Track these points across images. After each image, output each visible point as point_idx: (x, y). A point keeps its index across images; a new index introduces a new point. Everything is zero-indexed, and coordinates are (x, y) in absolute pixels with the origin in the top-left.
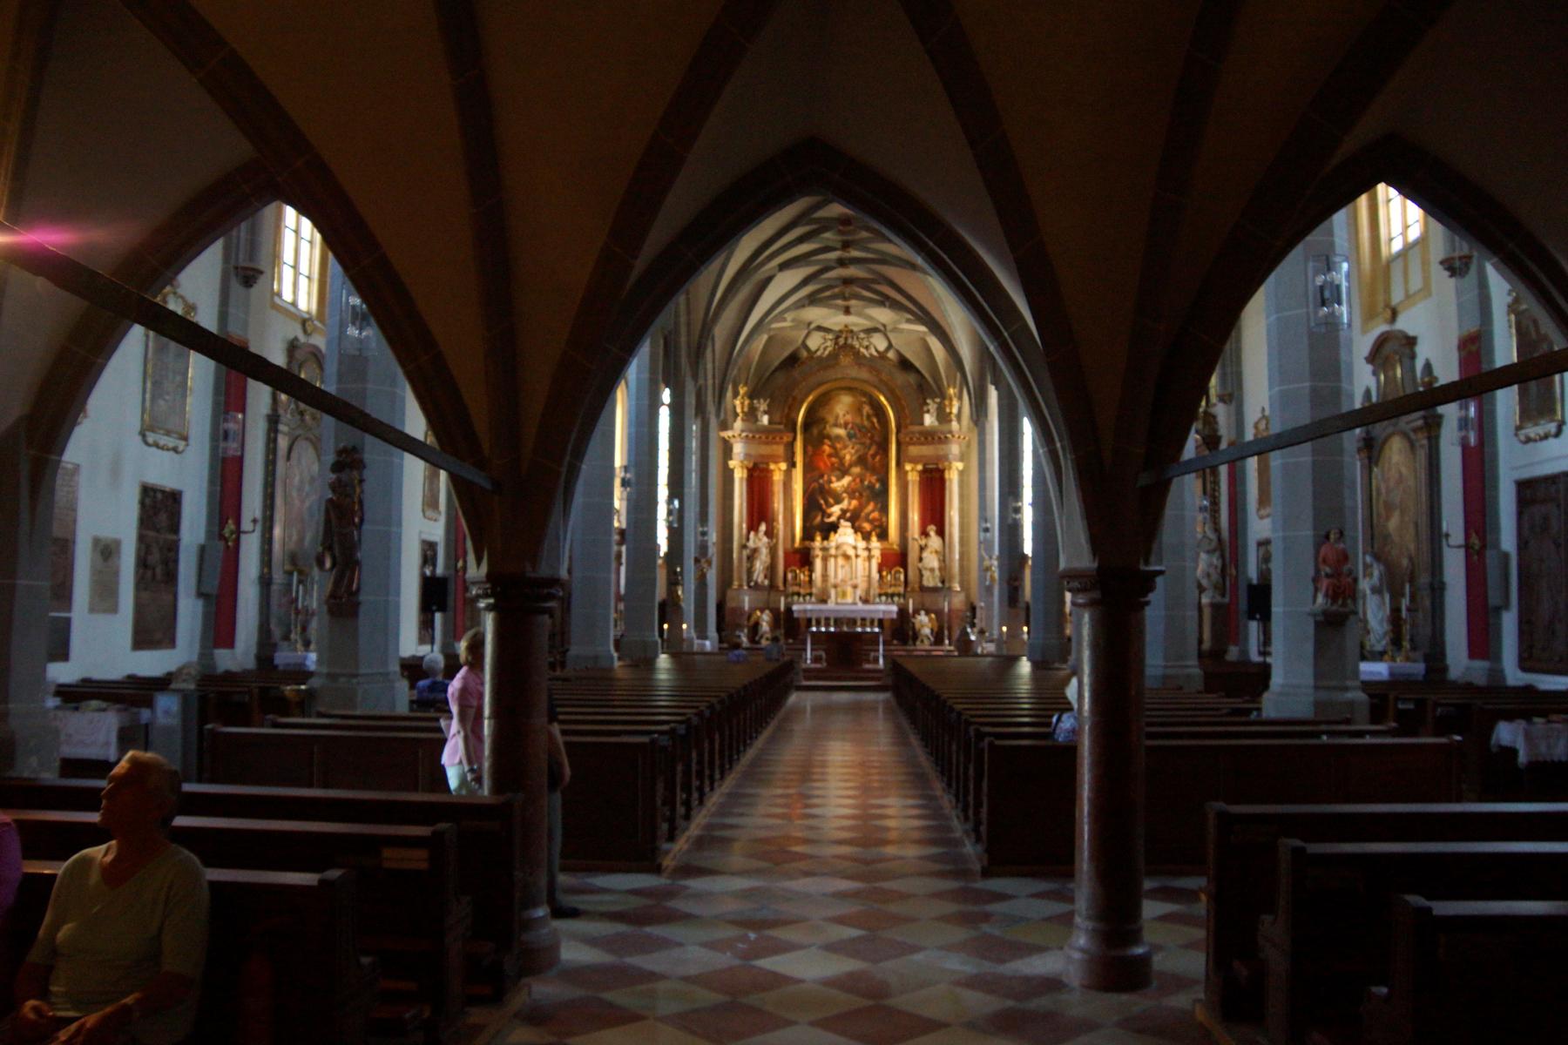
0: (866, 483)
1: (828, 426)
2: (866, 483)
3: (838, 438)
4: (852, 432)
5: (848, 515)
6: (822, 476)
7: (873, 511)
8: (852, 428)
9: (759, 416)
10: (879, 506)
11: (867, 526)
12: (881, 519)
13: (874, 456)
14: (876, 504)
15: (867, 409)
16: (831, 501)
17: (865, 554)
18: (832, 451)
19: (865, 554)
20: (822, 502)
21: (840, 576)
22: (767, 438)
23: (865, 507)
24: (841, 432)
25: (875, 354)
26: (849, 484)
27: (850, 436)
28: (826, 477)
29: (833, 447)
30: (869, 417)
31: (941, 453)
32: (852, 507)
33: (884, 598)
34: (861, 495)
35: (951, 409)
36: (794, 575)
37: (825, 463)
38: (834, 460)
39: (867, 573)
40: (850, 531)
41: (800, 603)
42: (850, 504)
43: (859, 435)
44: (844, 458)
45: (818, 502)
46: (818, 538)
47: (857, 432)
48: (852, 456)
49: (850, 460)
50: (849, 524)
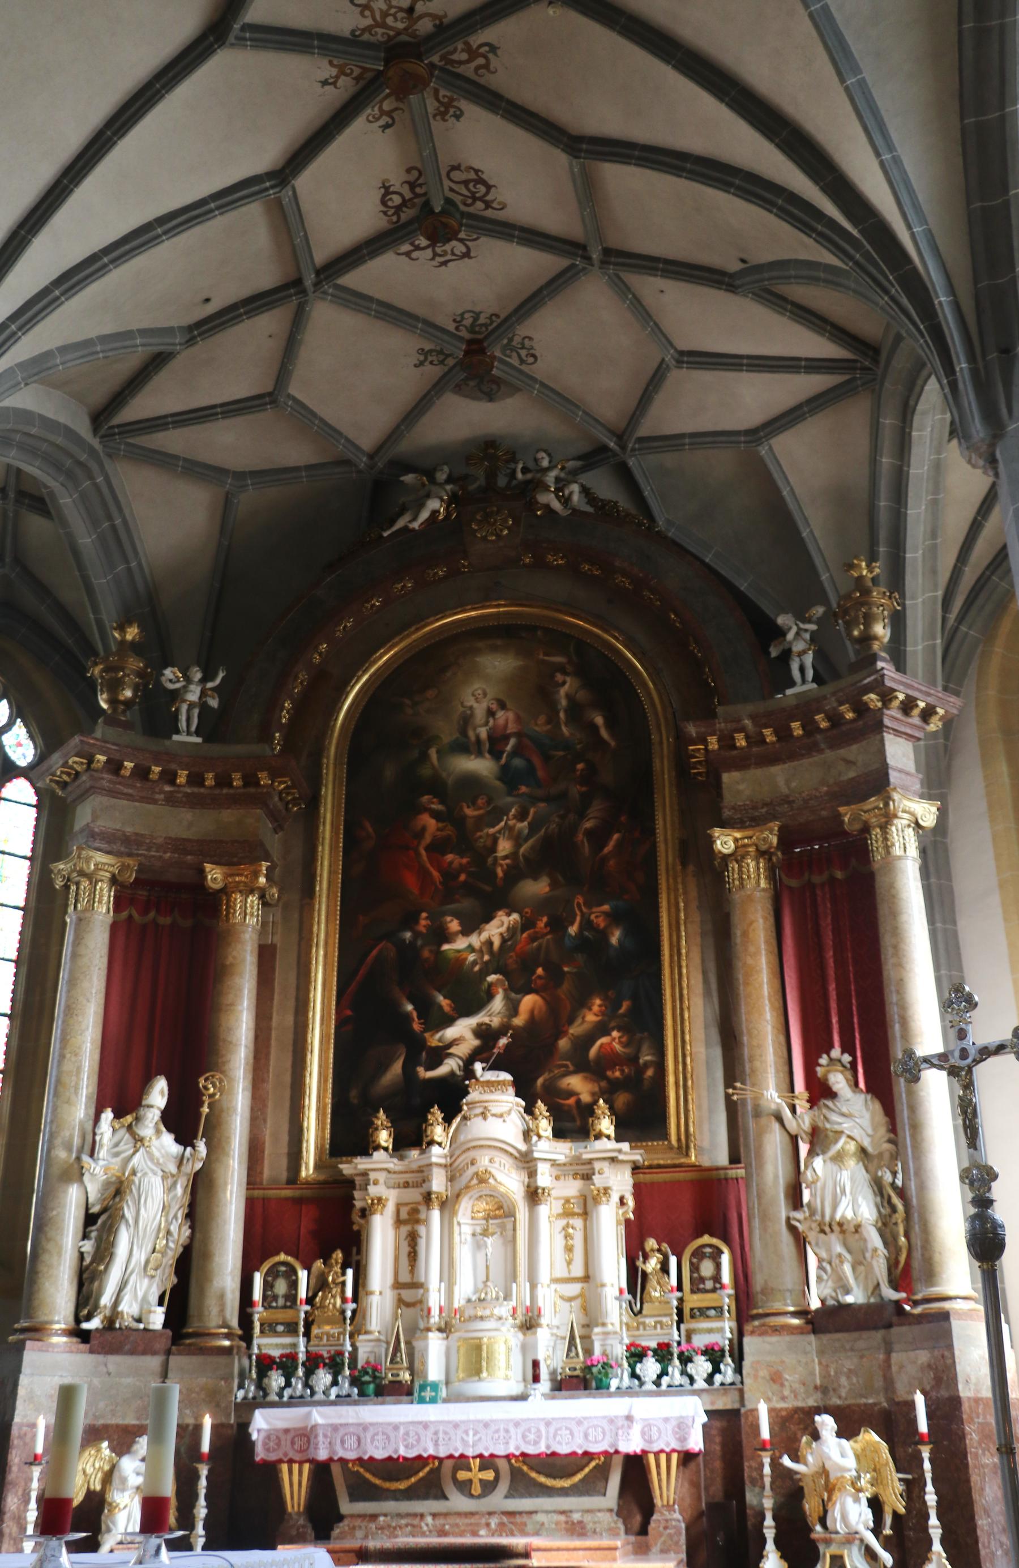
0: (573, 930)
1: (433, 753)
2: (573, 930)
3: (471, 783)
4: (518, 762)
5: (503, 1041)
6: (410, 920)
7: (602, 1029)
8: (516, 752)
9: (183, 724)
10: (625, 1006)
11: (577, 1084)
12: (633, 1060)
13: (598, 836)
14: (612, 1006)
15: (567, 688)
16: (443, 1002)
17: (572, 1188)
18: (449, 831)
19: (572, 1188)
20: (410, 1007)
21: (465, 1288)
22: (197, 779)
23: (571, 1021)
24: (481, 766)
25: (589, 509)
26: (509, 938)
27: (508, 777)
28: (424, 922)
29: (450, 817)
30: (575, 710)
31: (852, 774)
32: (518, 1021)
33: (650, 1367)
34: (555, 975)
35: (869, 620)
36: (281, 1287)
37: (424, 875)
38: (450, 857)
39: (578, 1271)
40: (509, 1101)
41: (294, 1401)
42: (513, 1009)
43: (540, 774)
44: (493, 848)
45: (397, 1006)
46: (384, 1137)
47: (537, 761)
48: (518, 840)
49: (513, 855)
50: (506, 1076)
